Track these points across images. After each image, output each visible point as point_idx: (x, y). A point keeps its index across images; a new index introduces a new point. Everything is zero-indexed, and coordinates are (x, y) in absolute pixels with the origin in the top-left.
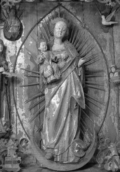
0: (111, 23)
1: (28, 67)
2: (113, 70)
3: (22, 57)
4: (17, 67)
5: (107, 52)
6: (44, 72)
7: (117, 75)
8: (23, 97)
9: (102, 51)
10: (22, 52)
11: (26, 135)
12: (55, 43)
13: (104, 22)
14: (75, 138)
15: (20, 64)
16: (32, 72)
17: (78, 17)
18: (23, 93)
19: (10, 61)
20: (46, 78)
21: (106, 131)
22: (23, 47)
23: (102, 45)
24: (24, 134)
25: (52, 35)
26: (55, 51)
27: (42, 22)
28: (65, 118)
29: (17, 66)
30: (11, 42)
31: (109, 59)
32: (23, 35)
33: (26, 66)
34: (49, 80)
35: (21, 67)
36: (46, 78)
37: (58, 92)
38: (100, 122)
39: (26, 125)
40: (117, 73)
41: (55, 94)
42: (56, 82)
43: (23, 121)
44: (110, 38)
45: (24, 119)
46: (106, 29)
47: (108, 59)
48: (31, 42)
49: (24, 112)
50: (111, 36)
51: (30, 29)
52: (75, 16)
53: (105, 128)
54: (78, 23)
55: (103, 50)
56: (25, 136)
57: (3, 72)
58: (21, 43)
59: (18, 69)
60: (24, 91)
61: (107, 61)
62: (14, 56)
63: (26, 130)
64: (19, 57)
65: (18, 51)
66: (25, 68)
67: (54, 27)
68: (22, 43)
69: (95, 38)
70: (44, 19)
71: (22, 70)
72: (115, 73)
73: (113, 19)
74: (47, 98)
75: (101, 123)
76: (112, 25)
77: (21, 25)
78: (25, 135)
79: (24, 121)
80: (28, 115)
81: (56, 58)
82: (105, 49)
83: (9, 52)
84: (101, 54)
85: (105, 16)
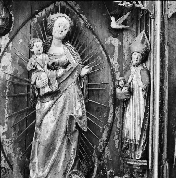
0: (121, 27)
1: (16, 72)
2: (121, 84)
3: (8, 58)
5: (114, 61)
6: (37, 81)
7: (126, 91)
8: (6, 111)
9: (109, 60)
10: (8, 52)
11: (6, 162)
12: (53, 45)
13: (114, 24)
14: (72, 169)
16: (19, 79)
17: (82, 15)
18: (5, 105)
20: (39, 90)
21: (108, 158)
22: (10, 45)
23: (109, 52)
24: (3, 160)
25: (51, 34)
26: (52, 55)
27: (37, 16)
28: (60, 143)
31: (116, 69)
32: (11, 30)
34: (42, 92)
35: (5, 72)
36: (39, 90)
37: (53, 108)
38: (101, 147)
39: (7, 148)
41: (49, 110)
42: (53, 95)
43: (3, 142)
44: (119, 44)
45: (5, 140)
46: (115, 34)
47: (116, 70)
48: (20, 39)
49: (6, 130)
50: (120, 43)
51: (21, 22)
52: (79, 14)
53: (108, 156)
54: (82, 22)
55: (110, 58)
56: (5, 162)
58: (9, 39)
60: (7, 103)
61: (114, 72)
63: (6, 154)
66: (10, 73)
67: (53, 24)
68: (10, 39)
69: (100, 43)
70: (39, 13)
71: (7, 75)
72: (124, 89)
73: (124, 23)
74: (39, 116)
75: (103, 147)
76: (123, 29)
77: (11, 15)
78: (5, 161)
79: (4, 142)
80: (11, 133)
81: (53, 64)
82: (112, 57)
84: (106, 64)
85: (114, 17)
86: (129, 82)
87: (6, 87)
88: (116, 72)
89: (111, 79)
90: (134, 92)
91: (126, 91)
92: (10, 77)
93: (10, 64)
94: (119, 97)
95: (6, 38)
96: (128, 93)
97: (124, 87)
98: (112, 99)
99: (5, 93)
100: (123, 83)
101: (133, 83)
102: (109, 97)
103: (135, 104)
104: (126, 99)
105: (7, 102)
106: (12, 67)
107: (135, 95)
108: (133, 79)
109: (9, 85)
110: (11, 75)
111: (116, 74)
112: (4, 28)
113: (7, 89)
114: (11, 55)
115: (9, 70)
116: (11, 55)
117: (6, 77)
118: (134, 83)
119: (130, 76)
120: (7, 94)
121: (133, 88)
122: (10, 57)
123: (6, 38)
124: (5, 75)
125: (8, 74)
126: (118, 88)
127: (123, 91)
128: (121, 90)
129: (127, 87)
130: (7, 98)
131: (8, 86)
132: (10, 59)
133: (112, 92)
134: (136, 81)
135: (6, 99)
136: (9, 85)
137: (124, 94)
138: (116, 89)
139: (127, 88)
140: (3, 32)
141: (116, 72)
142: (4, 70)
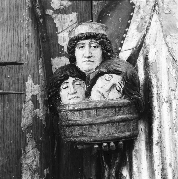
7: (114, 96)
40: (117, 79)
61: (49, 12)
72: (102, 84)
86: (125, 55)
88: (58, 11)
89: (32, 41)
90: (155, 103)
91: (114, 96)
94: (77, 131)
96: (124, 105)
97: (101, 74)
98: (38, 147)
100: (98, 53)
101: (146, 59)
102: (22, 135)
103: (163, 169)
104: (116, 143)
107: (160, 118)
108: (147, 41)
111: (58, 19)
118: (151, 58)
119: (128, 25)
121: (148, 84)
126: (70, 80)
127: (95, 96)
128: (88, 94)
129: (117, 73)
133: (40, 113)
134: (165, 48)
137: (103, 114)
138: (58, 90)
139: (117, 79)
141: (58, 11)
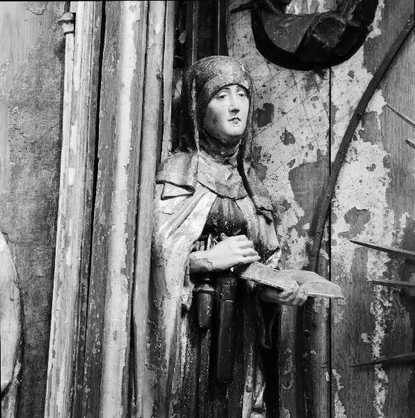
3: (372, 168)
4: (334, 236)
15: (358, 217)
18: (374, 409)
19: (289, 195)
22: (377, 103)
29: (334, 226)
30: (300, 76)
32: (376, 32)
33: (397, 226)
57: (242, 267)
58: (365, 77)
59: (342, 250)
60: (381, 397)
62: (316, 164)
64: (351, 174)
65: (340, 130)
66: (387, 242)
68: (370, 76)
71: (371, 256)
83: (288, 138)
87: (373, 318)
92: (387, 264)
93: (383, 198)
95: (351, 74)
99: (369, 347)
105: (383, 393)
106: (392, 214)
109: (387, 304)
110: (391, 253)
112: (338, 24)
113: (378, 328)
114: (384, 154)
115: (379, 230)
116: (384, 154)
117: (369, 265)
120: (376, 351)
122: (380, 165)
123: (351, 74)
124: (364, 259)
125: (379, 249)
130: (381, 375)
131: (380, 312)
132: (381, 171)
135: (374, 378)
136: (387, 304)
140: (336, 41)
142: (357, 230)
